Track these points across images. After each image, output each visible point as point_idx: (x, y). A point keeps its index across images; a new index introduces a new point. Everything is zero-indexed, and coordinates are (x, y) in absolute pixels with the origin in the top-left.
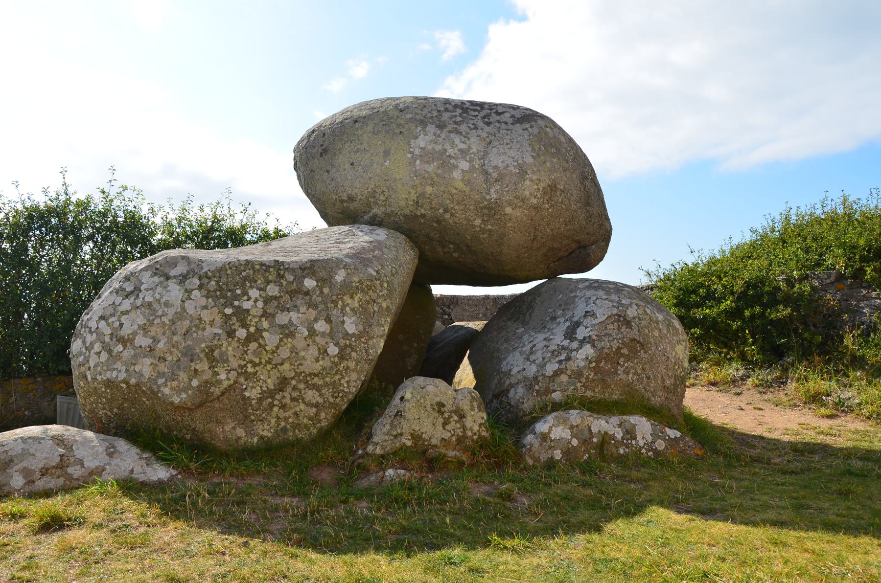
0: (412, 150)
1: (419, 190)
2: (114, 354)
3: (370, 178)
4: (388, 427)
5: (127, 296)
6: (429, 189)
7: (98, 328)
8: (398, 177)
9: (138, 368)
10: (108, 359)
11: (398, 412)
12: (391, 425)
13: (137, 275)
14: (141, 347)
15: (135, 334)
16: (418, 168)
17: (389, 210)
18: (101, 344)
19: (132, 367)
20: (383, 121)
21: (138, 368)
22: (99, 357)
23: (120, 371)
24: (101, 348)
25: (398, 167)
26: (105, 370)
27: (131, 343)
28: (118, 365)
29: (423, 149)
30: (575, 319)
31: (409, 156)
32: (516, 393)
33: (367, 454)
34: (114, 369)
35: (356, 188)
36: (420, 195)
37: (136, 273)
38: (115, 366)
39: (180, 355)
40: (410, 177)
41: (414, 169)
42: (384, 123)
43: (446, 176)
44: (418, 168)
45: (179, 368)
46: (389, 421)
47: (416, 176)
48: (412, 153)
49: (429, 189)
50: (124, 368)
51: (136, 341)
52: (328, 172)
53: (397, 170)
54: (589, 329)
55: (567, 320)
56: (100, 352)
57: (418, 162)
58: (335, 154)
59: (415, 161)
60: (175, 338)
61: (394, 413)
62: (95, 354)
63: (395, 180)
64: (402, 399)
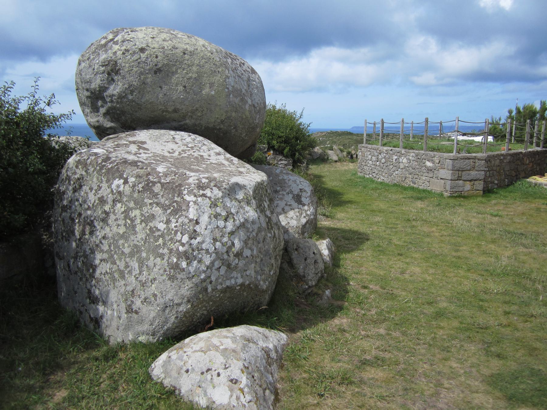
0: (228, 86)
1: (229, 114)
2: (232, 266)
3: (198, 100)
4: (314, 270)
5: (226, 220)
6: (234, 114)
7: (215, 249)
8: (219, 104)
9: (248, 273)
10: (226, 271)
11: (315, 261)
12: (315, 269)
13: (221, 201)
14: (247, 257)
15: (242, 249)
16: (231, 100)
17: (198, 122)
18: (221, 262)
19: (245, 273)
20: (204, 59)
21: (248, 273)
22: (219, 271)
23: (237, 278)
24: (221, 264)
25: (219, 97)
26: (224, 281)
27: (241, 256)
28: (234, 274)
29: (233, 87)
30: (296, 193)
31: (227, 90)
32: (289, 236)
33: (309, 287)
34: (232, 278)
35: (184, 105)
36: (228, 117)
37: (218, 199)
38: (232, 275)
39: (262, 256)
40: (226, 105)
41: (229, 100)
42: (206, 61)
43: (244, 107)
44: (231, 100)
45: (264, 265)
46: (313, 267)
47: (230, 105)
48: (228, 88)
49: (234, 114)
50: (239, 275)
51: (244, 253)
52: (161, 87)
53: (218, 99)
54: (308, 199)
55: (289, 194)
56: (220, 268)
57: (231, 96)
58: (168, 75)
59: (230, 95)
60: (260, 245)
61: (313, 262)
62: (216, 270)
63: (217, 105)
64: (314, 253)
